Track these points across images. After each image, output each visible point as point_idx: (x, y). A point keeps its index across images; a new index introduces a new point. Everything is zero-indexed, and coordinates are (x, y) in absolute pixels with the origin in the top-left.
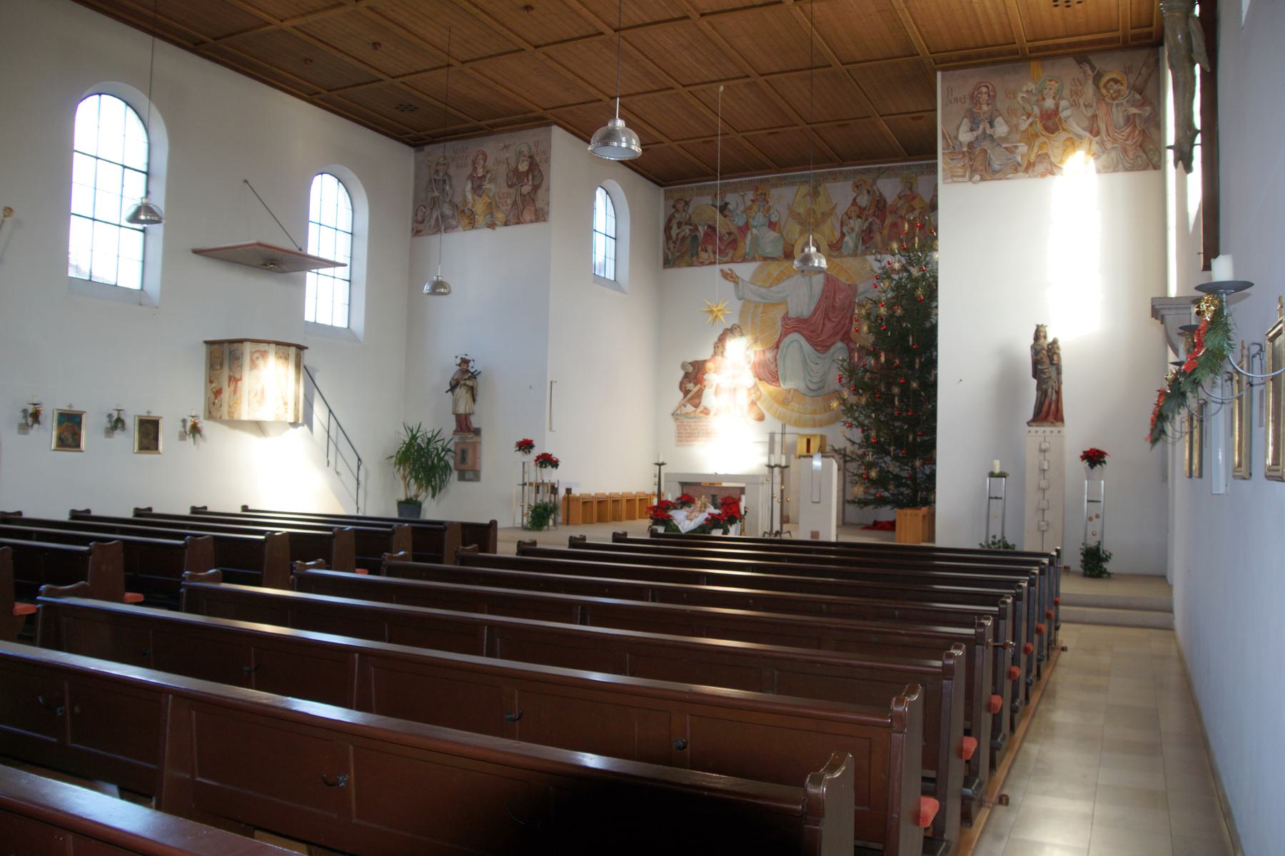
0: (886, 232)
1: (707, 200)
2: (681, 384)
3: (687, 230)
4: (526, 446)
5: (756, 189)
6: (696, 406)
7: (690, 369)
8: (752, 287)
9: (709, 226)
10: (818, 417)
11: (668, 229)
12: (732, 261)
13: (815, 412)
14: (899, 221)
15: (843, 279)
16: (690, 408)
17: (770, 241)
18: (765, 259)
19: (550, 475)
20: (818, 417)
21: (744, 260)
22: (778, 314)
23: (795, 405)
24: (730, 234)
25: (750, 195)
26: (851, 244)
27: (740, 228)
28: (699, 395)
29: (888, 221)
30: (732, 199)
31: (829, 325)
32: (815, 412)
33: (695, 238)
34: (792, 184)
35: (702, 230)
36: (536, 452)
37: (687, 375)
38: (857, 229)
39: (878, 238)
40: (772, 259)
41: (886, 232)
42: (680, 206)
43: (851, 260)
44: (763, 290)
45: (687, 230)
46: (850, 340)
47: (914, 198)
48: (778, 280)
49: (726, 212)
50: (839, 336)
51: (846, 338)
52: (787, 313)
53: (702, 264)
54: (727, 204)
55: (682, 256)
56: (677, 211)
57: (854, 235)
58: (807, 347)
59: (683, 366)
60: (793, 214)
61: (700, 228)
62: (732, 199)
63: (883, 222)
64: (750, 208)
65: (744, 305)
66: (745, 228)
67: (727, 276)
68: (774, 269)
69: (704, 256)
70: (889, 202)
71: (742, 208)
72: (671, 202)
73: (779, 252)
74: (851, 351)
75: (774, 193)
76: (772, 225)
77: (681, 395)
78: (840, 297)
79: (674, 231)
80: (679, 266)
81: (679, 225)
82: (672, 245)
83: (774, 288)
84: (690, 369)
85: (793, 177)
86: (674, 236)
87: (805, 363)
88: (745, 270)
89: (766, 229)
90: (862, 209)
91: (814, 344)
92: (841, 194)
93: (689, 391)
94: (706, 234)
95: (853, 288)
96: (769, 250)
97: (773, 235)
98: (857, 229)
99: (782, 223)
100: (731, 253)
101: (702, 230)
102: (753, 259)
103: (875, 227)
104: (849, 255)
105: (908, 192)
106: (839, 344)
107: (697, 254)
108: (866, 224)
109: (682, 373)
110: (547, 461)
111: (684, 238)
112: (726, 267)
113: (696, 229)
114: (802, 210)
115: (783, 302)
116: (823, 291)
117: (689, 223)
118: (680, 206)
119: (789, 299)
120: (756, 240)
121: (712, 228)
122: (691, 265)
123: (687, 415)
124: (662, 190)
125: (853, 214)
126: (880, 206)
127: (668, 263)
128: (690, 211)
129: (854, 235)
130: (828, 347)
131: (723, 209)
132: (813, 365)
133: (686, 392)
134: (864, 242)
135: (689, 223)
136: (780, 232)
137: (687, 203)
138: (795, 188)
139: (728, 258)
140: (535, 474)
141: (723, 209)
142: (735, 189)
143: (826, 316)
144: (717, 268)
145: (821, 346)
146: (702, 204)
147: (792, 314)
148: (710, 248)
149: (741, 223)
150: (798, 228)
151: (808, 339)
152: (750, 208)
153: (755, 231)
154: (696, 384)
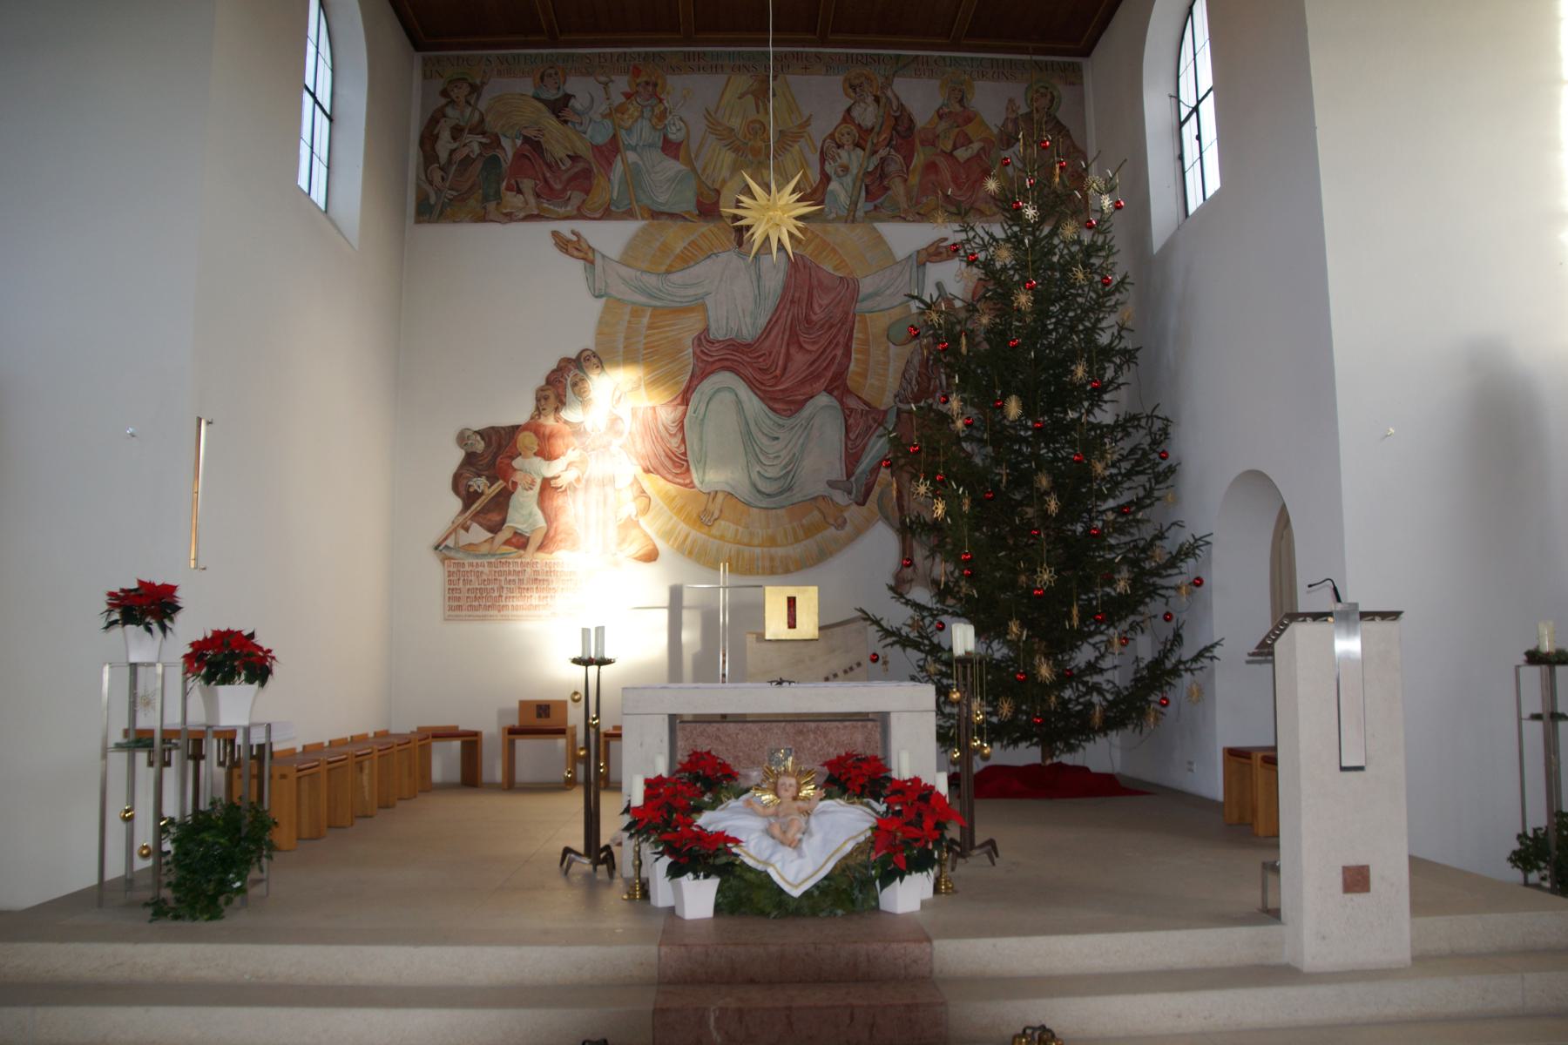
0: (914, 180)
1: (526, 86)
2: (458, 483)
3: (474, 144)
4: (147, 605)
5: (637, 72)
6: (495, 529)
7: (480, 446)
8: (624, 271)
9: (527, 140)
10: (780, 552)
11: (428, 139)
12: (580, 216)
13: (772, 541)
14: (943, 163)
15: (828, 267)
16: (478, 534)
17: (665, 179)
18: (655, 215)
19: (236, 705)
20: (780, 552)
21: (607, 214)
22: (688, 329)
23: (725, 526)
24: (574, 158)
25: (622, 83)
26: (843, 198)
27: (597, 149)
28: (502, 501)
29: (919, 159)
30: (581, 89)
31: (800, 359)
32: (772, 541)
33: (494, 161)
34: (716, 69)
35: (509, 147)
36: (190, 627)
37: (470, 459)
38: (854, 170)
39: (898, 188)
40: (672, 216)
41: (914, 180)
42: (460, 93)
43: (843, 228)
44: (651, 281)
45: (474, 144)
46: (847, 391)
47: (969, 120)
48: (686, 260)
49: (566, 114)
50: (823, 382)
51: (838, 386)
52: (707, 330)
53: (510, 217)
54: (568, 97)
56: (452, 102)
57: (848, 180)
58: (753, 403)
59: (462, 439)
61: (505, 143)
62: (581, 89)
63: (908, 159)
64: (621, 109)
65: (606, 310)
66: (610, 151)
67: (563, 244)
68: (677, 237)
69: (513, 200)
70: (921, 121)
71: (604, 108)
72: (439, 84)
73: (687, 203)
74: (847, 413)
75: (676, 85)
76: (671, 148)
77: (456, 504)
78: (822, 300)
79: (444, 146)
80: (454, 219)
81: (457, 132)
83: (675, 277)
84: (480, 446)
85: (718, 55)
86: (443, 156)
87: (748, 436)
88: (610, 237)
89: (657, 155)
90: (866, 132)
91: (768, 398)
92: (820, 98)
93: (478, 495)
94: (519, 156)
95: (850, 287)
97: (673, 167)
98: (854, 170)
99: (694, 147)
100: (576, 197)
101: (509, 147)
102: (629, 214)
103: (892, 168)
104: (838, 219)
105: (958, 108)
106: (823, 399)
107: (498, 196)
108: (875, 160)
109: (458, 455)
110: (230, 658)
111: (467, 161)
112: (565, 228)
114: (736, 123)
115: (699, 306)
116: (786, 288)
117: (479, 128)
118: (460, 93)
119: (709, 302)
120: (634, 177)
121: (534, 146)
122: (482, 218)
123: (470, 549)
124: (418, 57)
125: (846, 140)
126: (901, 129)
127: (427, 211)
128: (483, 105)
129: (848, 180)
130: (801, 404)
131: (560, 107)
132: (765, 441)
133: (469, 498)
134: (870, 196)
135: (479, 128)
136: (690, 163)
137: (475, 89)
138: (721, 79)
140: (177, 702)
141: (560, 107)
142: (587, 68)
143: (794, 340)
144: (543, 229)
145: (784, 400)
146: (511, 93)
147: (718, 332)
148: (527, 184)
149: (601, 138)
150: (728, 157)
151: (753, 385)
152: (621, 109)
153: (632, 157)
154: (492, 480)
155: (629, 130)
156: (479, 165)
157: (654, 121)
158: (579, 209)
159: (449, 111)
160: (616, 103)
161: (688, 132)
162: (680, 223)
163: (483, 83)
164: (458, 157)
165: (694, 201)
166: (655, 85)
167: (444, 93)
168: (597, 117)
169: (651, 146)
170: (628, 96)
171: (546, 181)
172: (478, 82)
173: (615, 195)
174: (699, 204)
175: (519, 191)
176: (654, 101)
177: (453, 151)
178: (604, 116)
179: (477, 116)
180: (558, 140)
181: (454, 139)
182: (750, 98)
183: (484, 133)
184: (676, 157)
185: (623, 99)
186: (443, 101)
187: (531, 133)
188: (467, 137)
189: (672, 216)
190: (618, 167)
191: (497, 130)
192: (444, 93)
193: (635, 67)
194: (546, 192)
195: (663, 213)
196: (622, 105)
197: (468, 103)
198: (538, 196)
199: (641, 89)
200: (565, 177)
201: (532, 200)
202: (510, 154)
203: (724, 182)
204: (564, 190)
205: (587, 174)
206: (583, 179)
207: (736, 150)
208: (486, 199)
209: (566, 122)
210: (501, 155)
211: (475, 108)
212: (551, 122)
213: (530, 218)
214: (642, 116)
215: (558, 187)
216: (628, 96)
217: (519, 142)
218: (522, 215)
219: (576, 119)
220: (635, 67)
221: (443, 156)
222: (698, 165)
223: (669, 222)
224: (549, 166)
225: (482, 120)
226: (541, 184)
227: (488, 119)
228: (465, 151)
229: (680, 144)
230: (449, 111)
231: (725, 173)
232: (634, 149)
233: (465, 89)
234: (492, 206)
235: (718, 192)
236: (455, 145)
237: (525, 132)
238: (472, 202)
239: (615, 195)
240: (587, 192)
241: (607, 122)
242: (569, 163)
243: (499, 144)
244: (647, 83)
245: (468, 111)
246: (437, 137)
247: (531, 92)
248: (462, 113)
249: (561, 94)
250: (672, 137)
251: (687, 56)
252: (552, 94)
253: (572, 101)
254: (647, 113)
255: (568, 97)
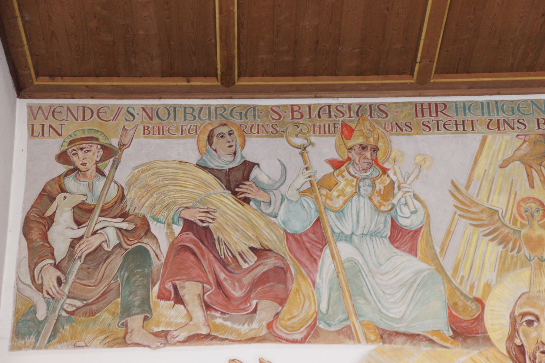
1: (187, 149)
3: (109, 231)
5: (347, 132)
9: (189, 225)
18: (386, 336)
24: (261, 252)
25: (326, 148)
27: (292, 238)
33: (140, 256)
34: (463, 126)
35: (163, 237)
40: (412, 337)
45: (109, 231)
49: (245, 189)
53: (164, 338)
54: (248, 167)
55: (90, 310)
60: (465, 205)
61: (156, 229)
62: (267, 154)
64: (326, 183)
66: (313, 241)
69: (168, 313)
71: (301, 181)
72: (55, 145)
75: (407, 150)
76: (402, 237)
79: (62, 233)
81: (82, 213)
82: (50, 277)
85: (466, 107)
86: (61, 249)
89: (384, 247)
94: (178, 249)
96: (397, 312)
97: (407, 265)
99: (438, 237)
100: (266, 309)
101: (163, 237)
102: (346, 334)
111: (98, 256)
113: (144, 228)
114: (499, 202)
117: (117, 208)
118: (89, 157)
120: (350, 281)
121: (200, 234)
128: (122, 176)
131: (237, 179)
136: (433, 259)
138: (472, 140)
139: (257, 326)
142: (275, 126)
148: (191, 290)
149: (300, 224)
150: (492, 251)
153: (345, 250)
155: (340, 212)
156: (117, 261)
157: (377, 199)
158: (270, 326)
159: (70, 183)
160: (319, 176)
161: (427, 216)
162: (425, 348)
163: (122, 146)
164: (84, 249)
165: (444, 315)
166: (375, 149)
167: (63, 157)
168: (292, 194)
169: (373, 234)
170: (337, 165)
171: (219, 285)
172: (115, 142)
173: (324, 307)
174: (453, 320)
175: (179, 300)
176: (374, 172)
177: (75, 242)
178: (303, 193)
179: (113, 192)
180: (235, 226)
181: (79, 223)
182: (518, 168)
183: (124, 216)
184: (413, 251)
185: (329, 169)
186: (62, 169)
187: (194, 216)
188: (97, 221)
189: (412, 337)
190: (326, 264)
191: (143, 212)
192: (63, 157)
193: (344, 125)
194: (219, 300)
195: (398, 334)
196: (326, 177)
197: (100, 172)
198: (208, 307)
199: (354, 155)
200: (247, 279)
201: (199, 314)
202: (165, 247)
203: (488, 287)
204: (246, 298)
205: (280, 274)
206: (275, 282)
207: (504, 241)
208: (127, 311)
209: (247, 200)
210: (148, 244)
211: (110, 179)
212: (224, 201)
213: (195, 339)
214: (357, 191)
215: (237, 293)
216: (337, 165)
217: (177, 229)
218: (183, 335)
219: (262, 197)
220: (344, 125)
221: (61, 249)
222: (448, 264)
223: (408, 347)
224: (224, 264)
225: (122, 197)
226: (211, 289)
227: (130, 196)
228: (95, 241)
229: (417, 232)
230: (70, 183)
231: (489, 275)
232: (349, 239)
233: (96, 153)
234: (135, 322)
235: (480, 302)
236: (79, 233)
237: (187, 215)
238: (105, 316)
239: (324, 307)
240: (282, 302)
241: (308, 201)
242: (252, 258)
243: (148, 231)
244: (363, 147)
245: (100, 183)
246: (51, 219)
247: (194, 157)
248: (91, 187)
249: (238, 162)
250: (403, 222)
251: (419, 109)
252: (224, 161)
253: (255, 172)
254: (366, 189)
255: (248, 167)
